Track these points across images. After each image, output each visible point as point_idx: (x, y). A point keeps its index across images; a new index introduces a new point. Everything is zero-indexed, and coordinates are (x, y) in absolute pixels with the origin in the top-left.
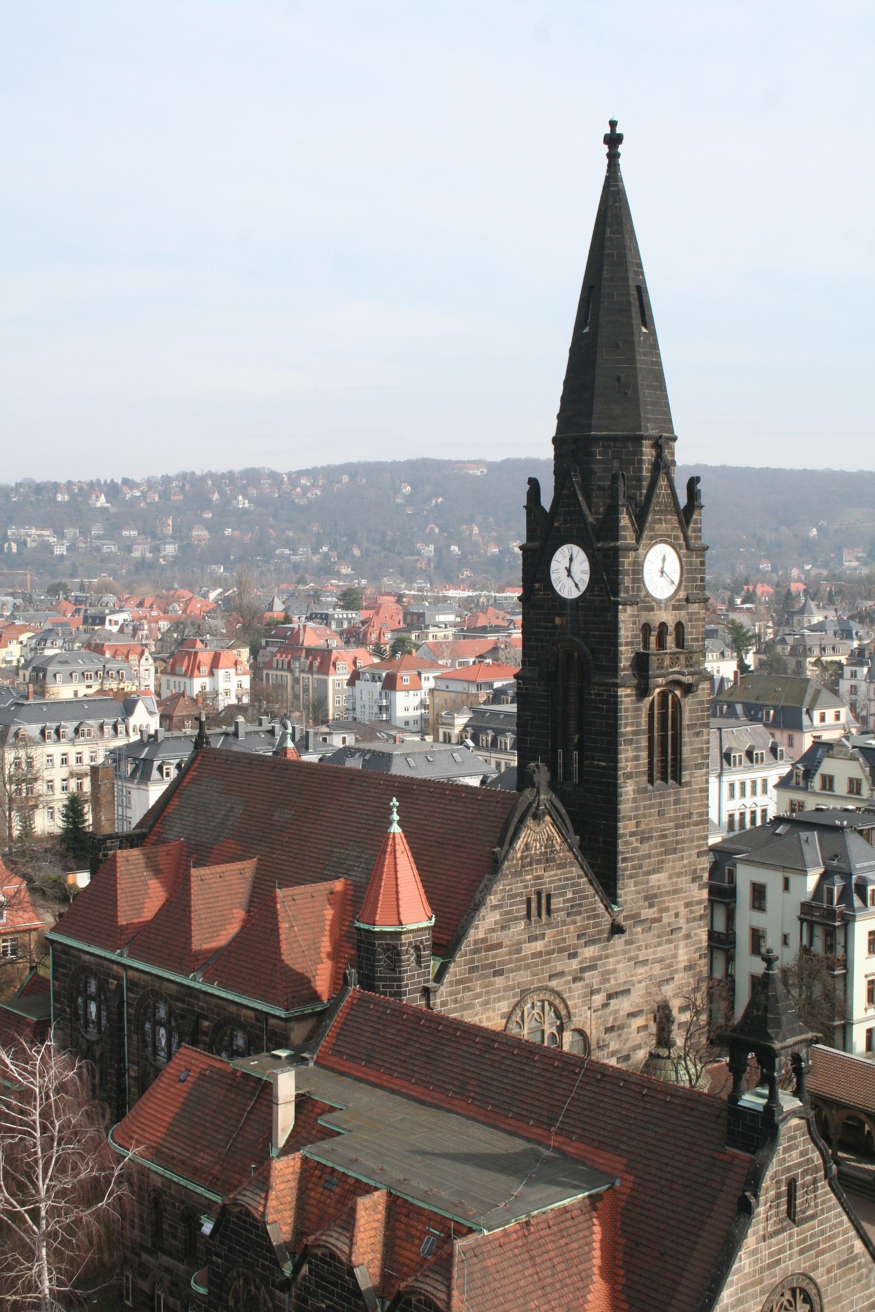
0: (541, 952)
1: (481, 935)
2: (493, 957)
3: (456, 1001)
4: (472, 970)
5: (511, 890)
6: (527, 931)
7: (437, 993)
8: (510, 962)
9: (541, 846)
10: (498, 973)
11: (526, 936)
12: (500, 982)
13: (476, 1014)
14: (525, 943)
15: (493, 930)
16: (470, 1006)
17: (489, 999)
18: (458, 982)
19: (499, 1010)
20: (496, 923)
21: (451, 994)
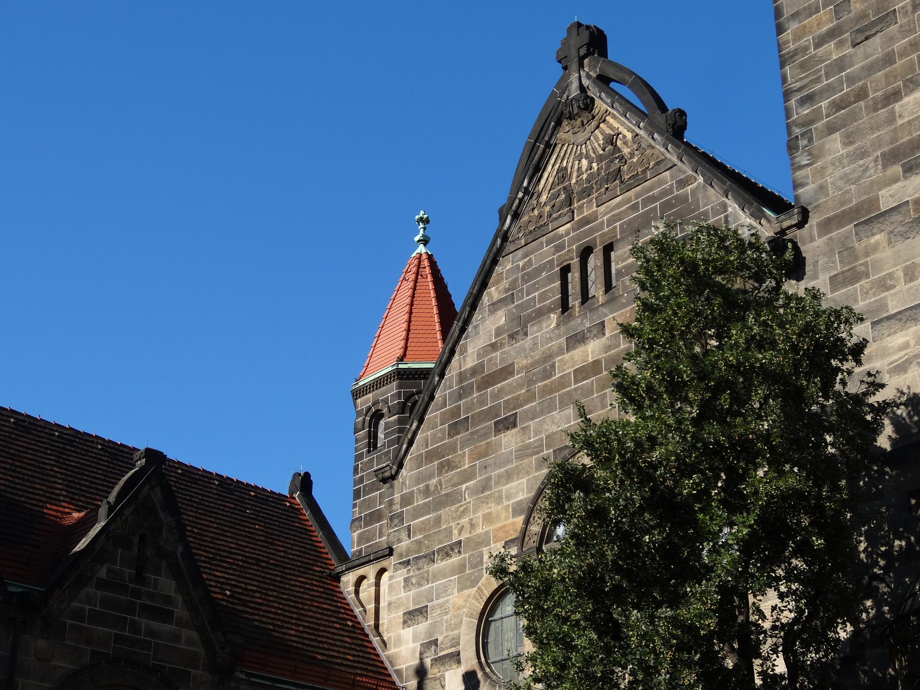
0: (596, 363)
1: (470, 362)
2: (495, 397)
3: (427, 492)
4: (454, 429)
5: (530, 263)
6: (562, 328)
7: (396, 482)
8: (530, 398)
9: (590, 163)
10: (508, 423)
11: (563, 340)
12: (510, 440)
13: (463, 512)
14: (560, 352)
15: (494, 347)
16: (451, 499)
17: (489, 479)
18: (430, 456)
19: (508, 498)
20: (499, 332)
21: (419, 480)
